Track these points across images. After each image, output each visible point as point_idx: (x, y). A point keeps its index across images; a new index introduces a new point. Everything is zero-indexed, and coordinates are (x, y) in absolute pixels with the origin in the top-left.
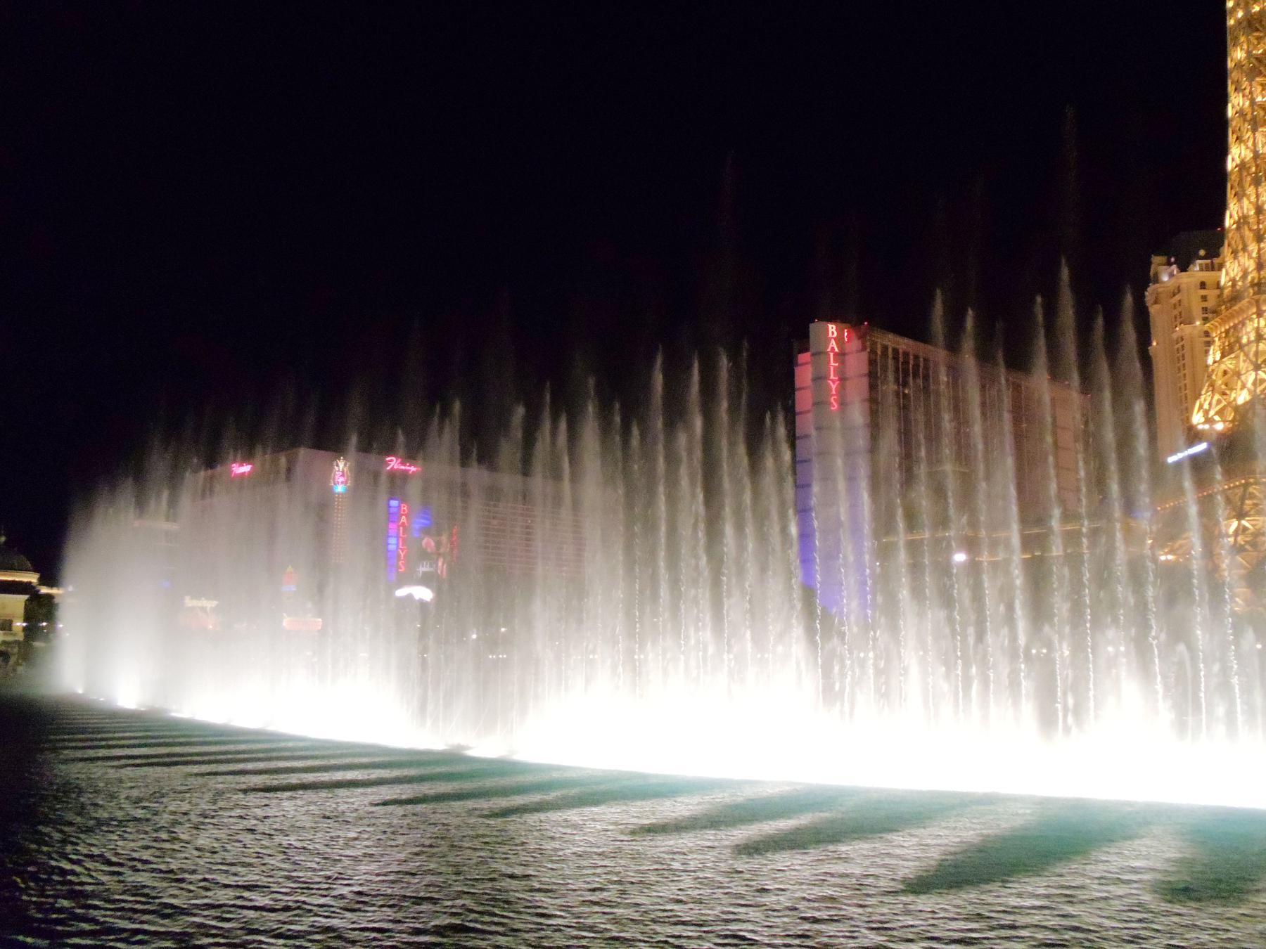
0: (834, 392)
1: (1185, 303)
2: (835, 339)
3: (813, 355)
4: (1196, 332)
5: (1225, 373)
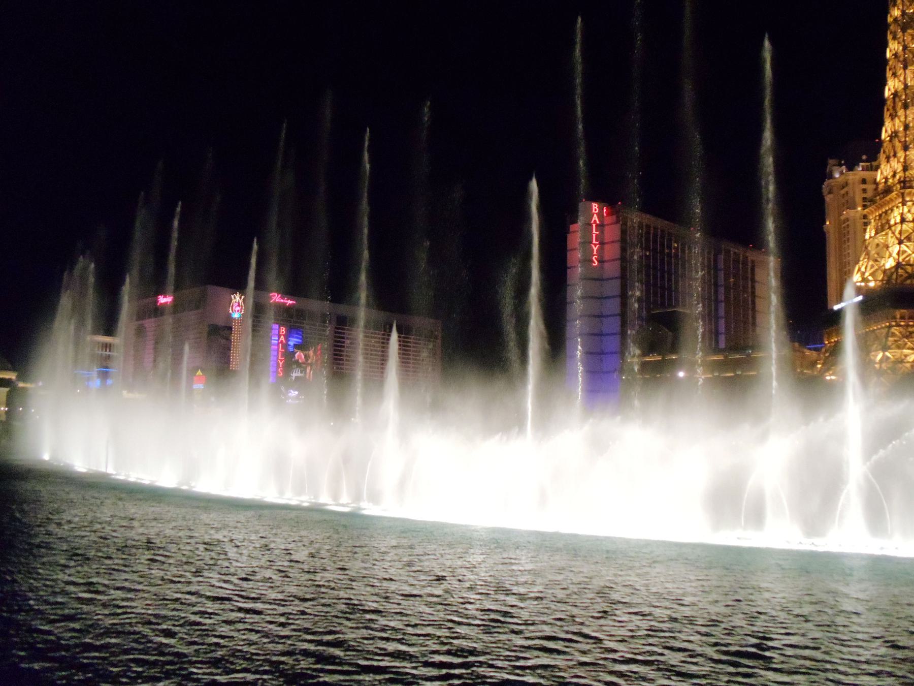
0: (595, 253)
1: (851, 194)
4: (858, 215)
5: (878, 245)
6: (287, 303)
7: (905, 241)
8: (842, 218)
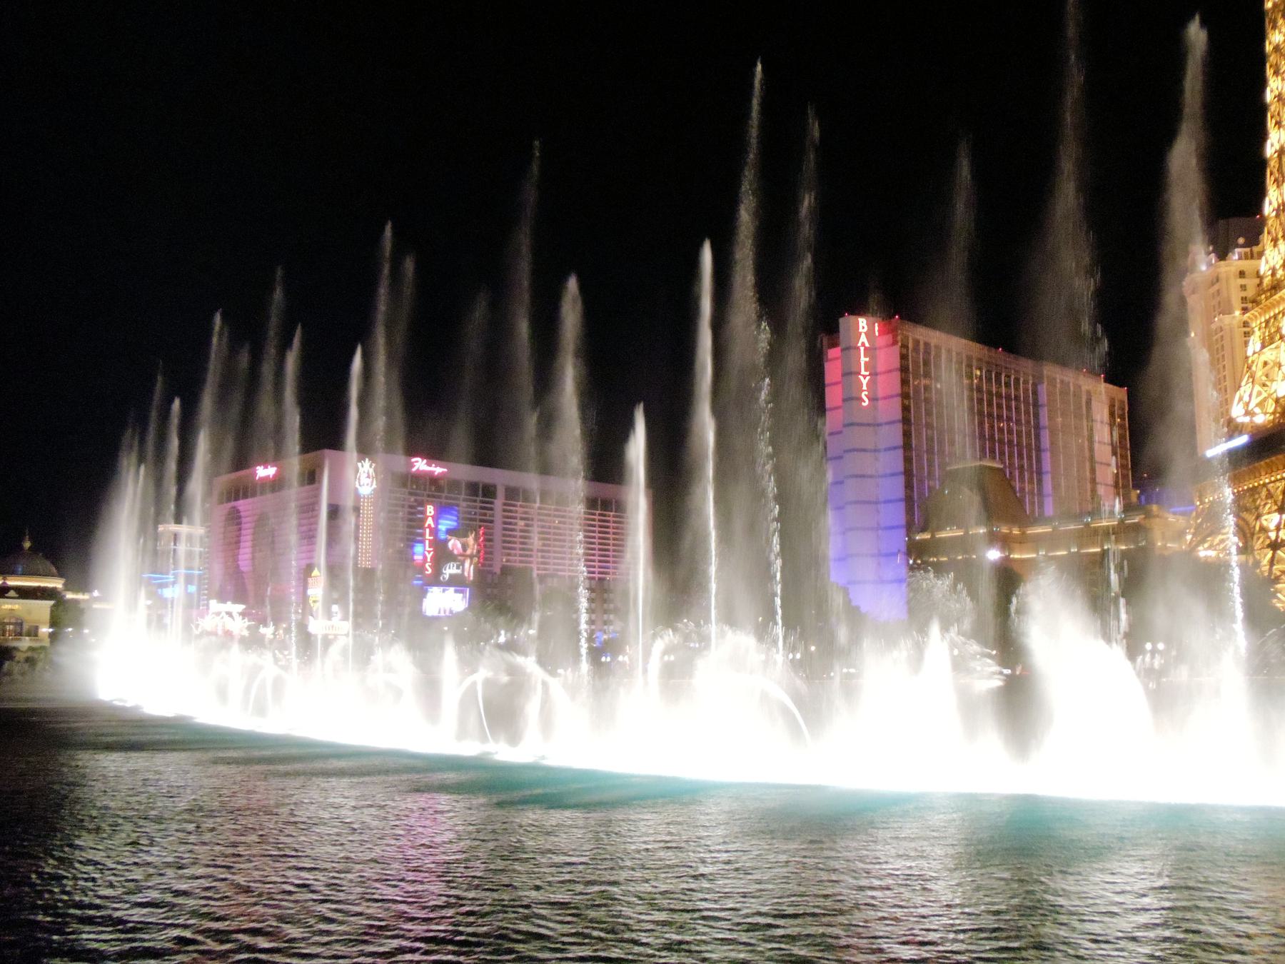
0: (865, 388)
1: (1224, 294)
2: (865, 333)
3: (842, 350)
4: (1235, 322)
5: (1265, 364)
6: (433, 472)
8: (1213, 327)
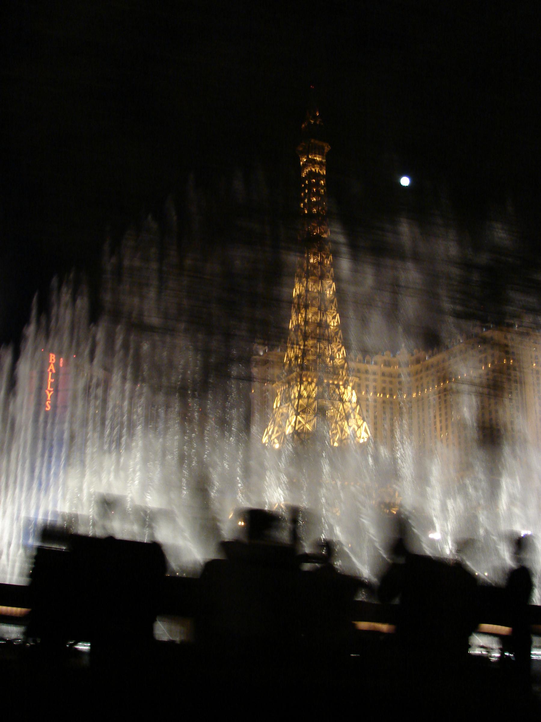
0: (49, 398)
2: (54, 364)
5: (282, 414)
7: (301, 413)
